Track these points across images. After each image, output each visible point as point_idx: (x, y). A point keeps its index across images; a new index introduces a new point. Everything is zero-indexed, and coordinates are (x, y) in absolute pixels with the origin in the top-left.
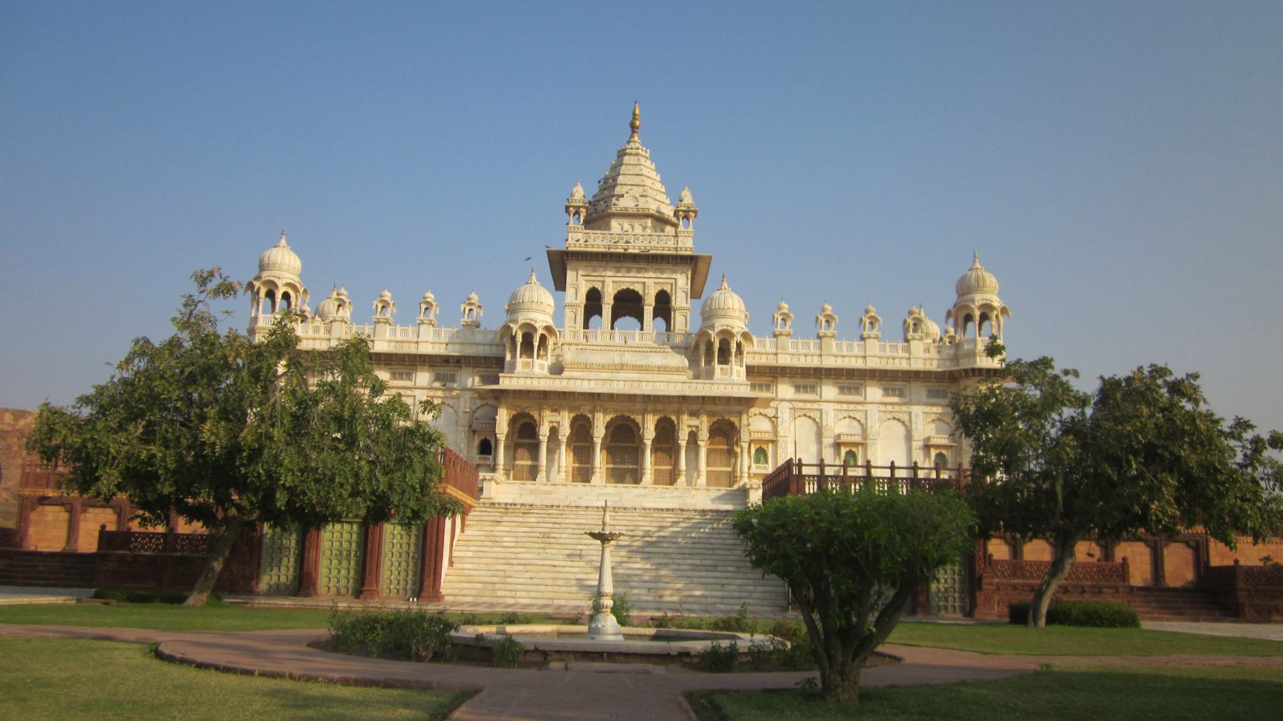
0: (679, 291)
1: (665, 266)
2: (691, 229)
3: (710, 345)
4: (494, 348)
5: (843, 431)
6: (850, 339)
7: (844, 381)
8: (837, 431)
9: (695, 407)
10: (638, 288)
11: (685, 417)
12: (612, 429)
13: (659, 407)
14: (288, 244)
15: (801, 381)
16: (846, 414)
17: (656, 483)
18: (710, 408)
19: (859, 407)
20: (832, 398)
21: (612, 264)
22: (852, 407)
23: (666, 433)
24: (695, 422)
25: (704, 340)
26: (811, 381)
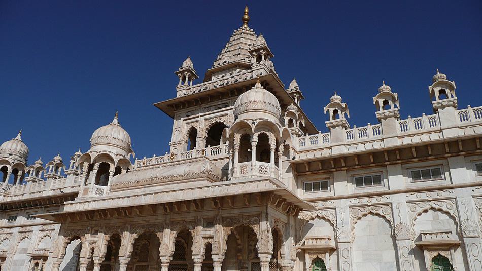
5: (428, 228)
6: (416, 114)
7: (416, 164)
8: (417, 230)
9: (210, 214)
14: (22, 138)
15: (363, 173)
16: (426, 206)
18: (225, 213)
19: (444, 194)
20: (403, 188)
21: (204, 106)
22: (433, 195)
24: (210, 232)
26: (373, 171)
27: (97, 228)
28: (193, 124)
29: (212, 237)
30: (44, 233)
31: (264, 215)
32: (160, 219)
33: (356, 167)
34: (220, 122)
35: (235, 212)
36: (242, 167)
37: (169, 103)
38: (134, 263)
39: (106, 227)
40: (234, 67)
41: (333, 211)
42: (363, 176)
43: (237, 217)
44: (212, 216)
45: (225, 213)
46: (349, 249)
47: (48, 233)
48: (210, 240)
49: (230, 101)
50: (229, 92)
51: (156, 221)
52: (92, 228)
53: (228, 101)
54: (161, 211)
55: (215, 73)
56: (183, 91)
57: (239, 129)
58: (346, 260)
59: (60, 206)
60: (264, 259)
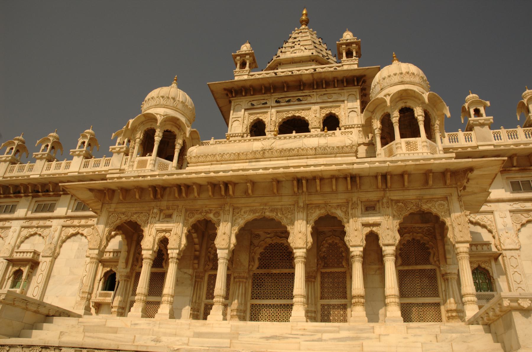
1: (330, 90)
3: (386, 121)
9: (373, 196)
10: (302, 114)
11: (358, 212)
12: (261, 250)
13: (317, 199)
15: (519, 177)
17: (311, 316)
23: (329, 236)
25: (379, 114)
27: (170, 212)
28: (258, 116)
29: (377, 225)
30: (30, 230)
31: (455, 198)
32: (287, 201)
33: (514, 169)
34: (299, 116)
35: (412, 195)
36: (408, 143)
37: (225, 86)
38: (205, 271)
39: (186, 210)
40: (310, 61)
41: (489, 216)
42: (519, 180)
43: (413, 201)
44: (375, 199)
45: (396, 195)
46: (517, 257)
47: (39, 231)
48: (375, 229)
49: (315, 93)
50: (315, 83)
51: (280, 203)
52: (161, 211)
53: (312, 94)
54: (287, 190)
55: (283, 64)
56: (242, 76)
57: (398, 100)
58: (515, 270)
59: (60, 195)
60: (461, 250)
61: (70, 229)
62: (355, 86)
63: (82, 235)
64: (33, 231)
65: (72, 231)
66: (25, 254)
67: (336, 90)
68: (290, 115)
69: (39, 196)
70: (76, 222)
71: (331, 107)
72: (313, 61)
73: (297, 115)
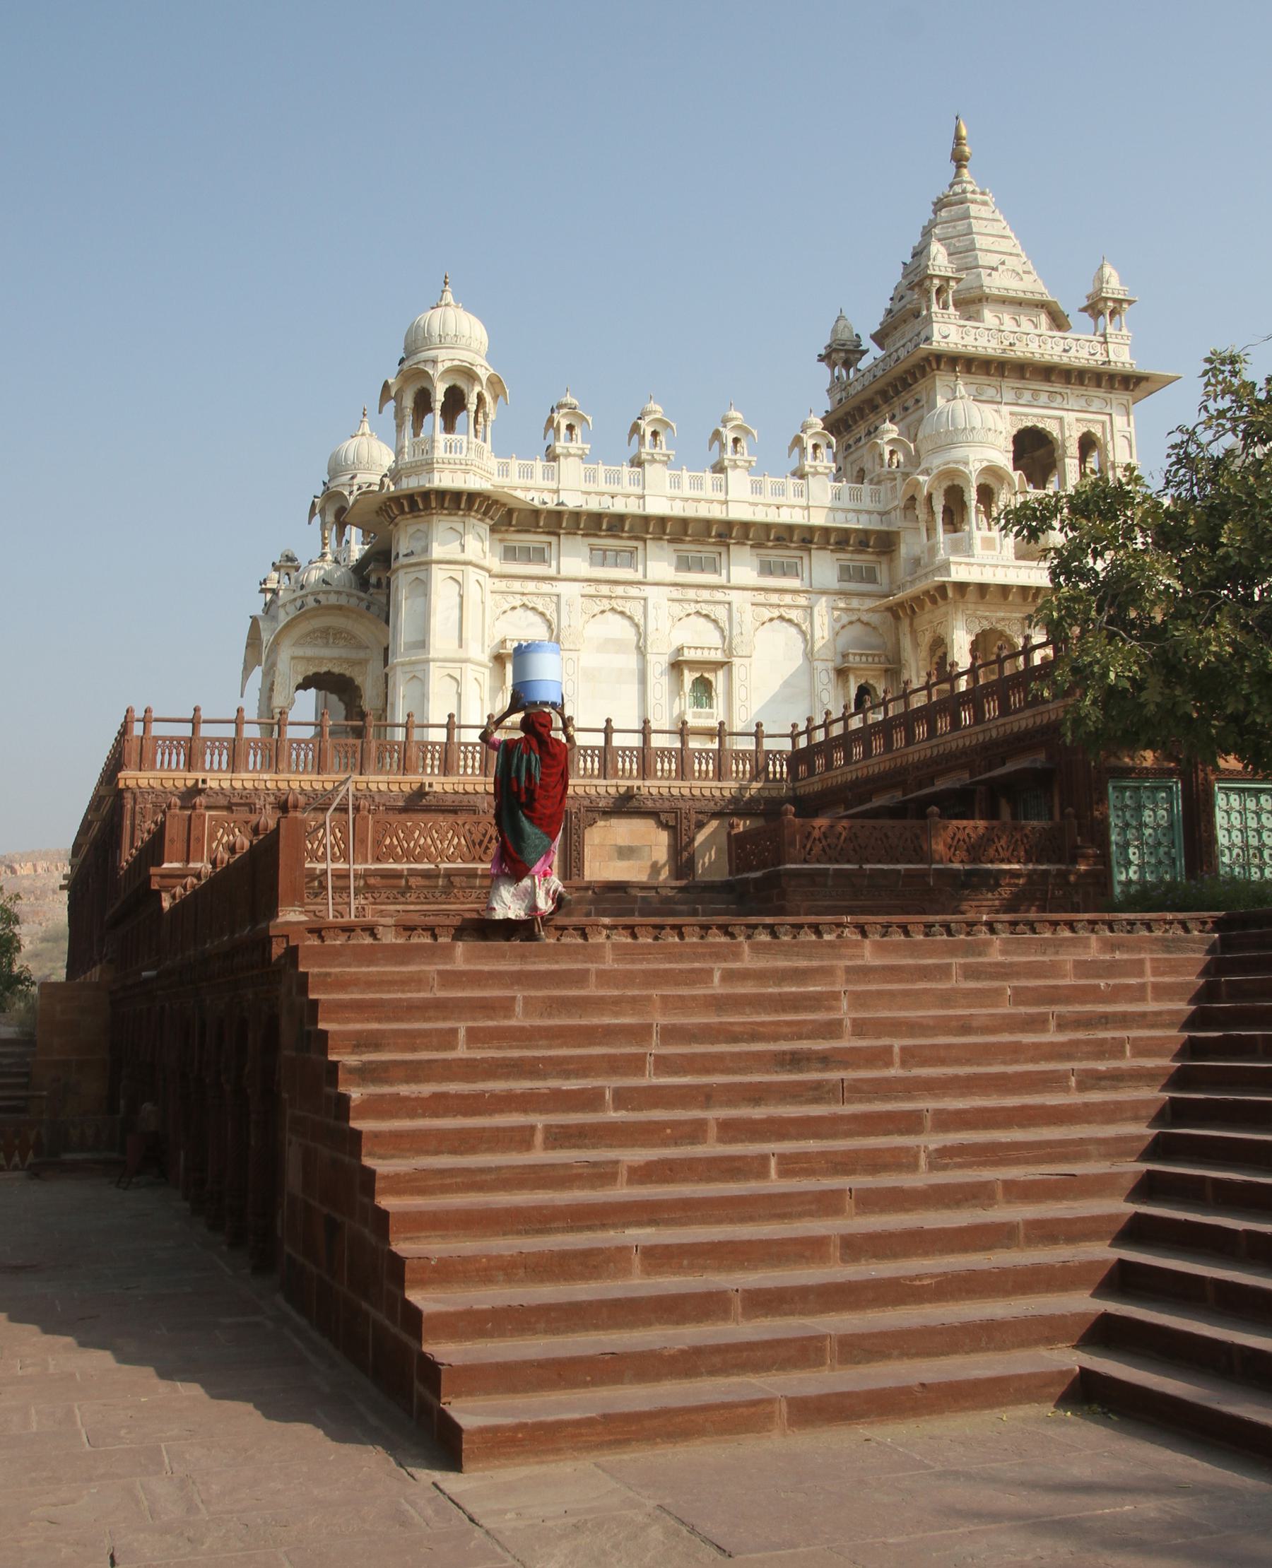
0: (1117, 436)
1: (1093, 391)
2: (1125, 332)
4: (864, 517)
10: (1052, 427)
40: (1037, 306)
61: (763, 609)
62: (1127, 389)
63: (790, 621)
64: (692, 608)
65: (767, 613)
66: (706, 651)
67: (1100, 392)
68: (1030, 424)
69: (681, 541)
70: (774, 598)
71: (1090, 421)
72: (1042, 307)
73: (1040, 425)
